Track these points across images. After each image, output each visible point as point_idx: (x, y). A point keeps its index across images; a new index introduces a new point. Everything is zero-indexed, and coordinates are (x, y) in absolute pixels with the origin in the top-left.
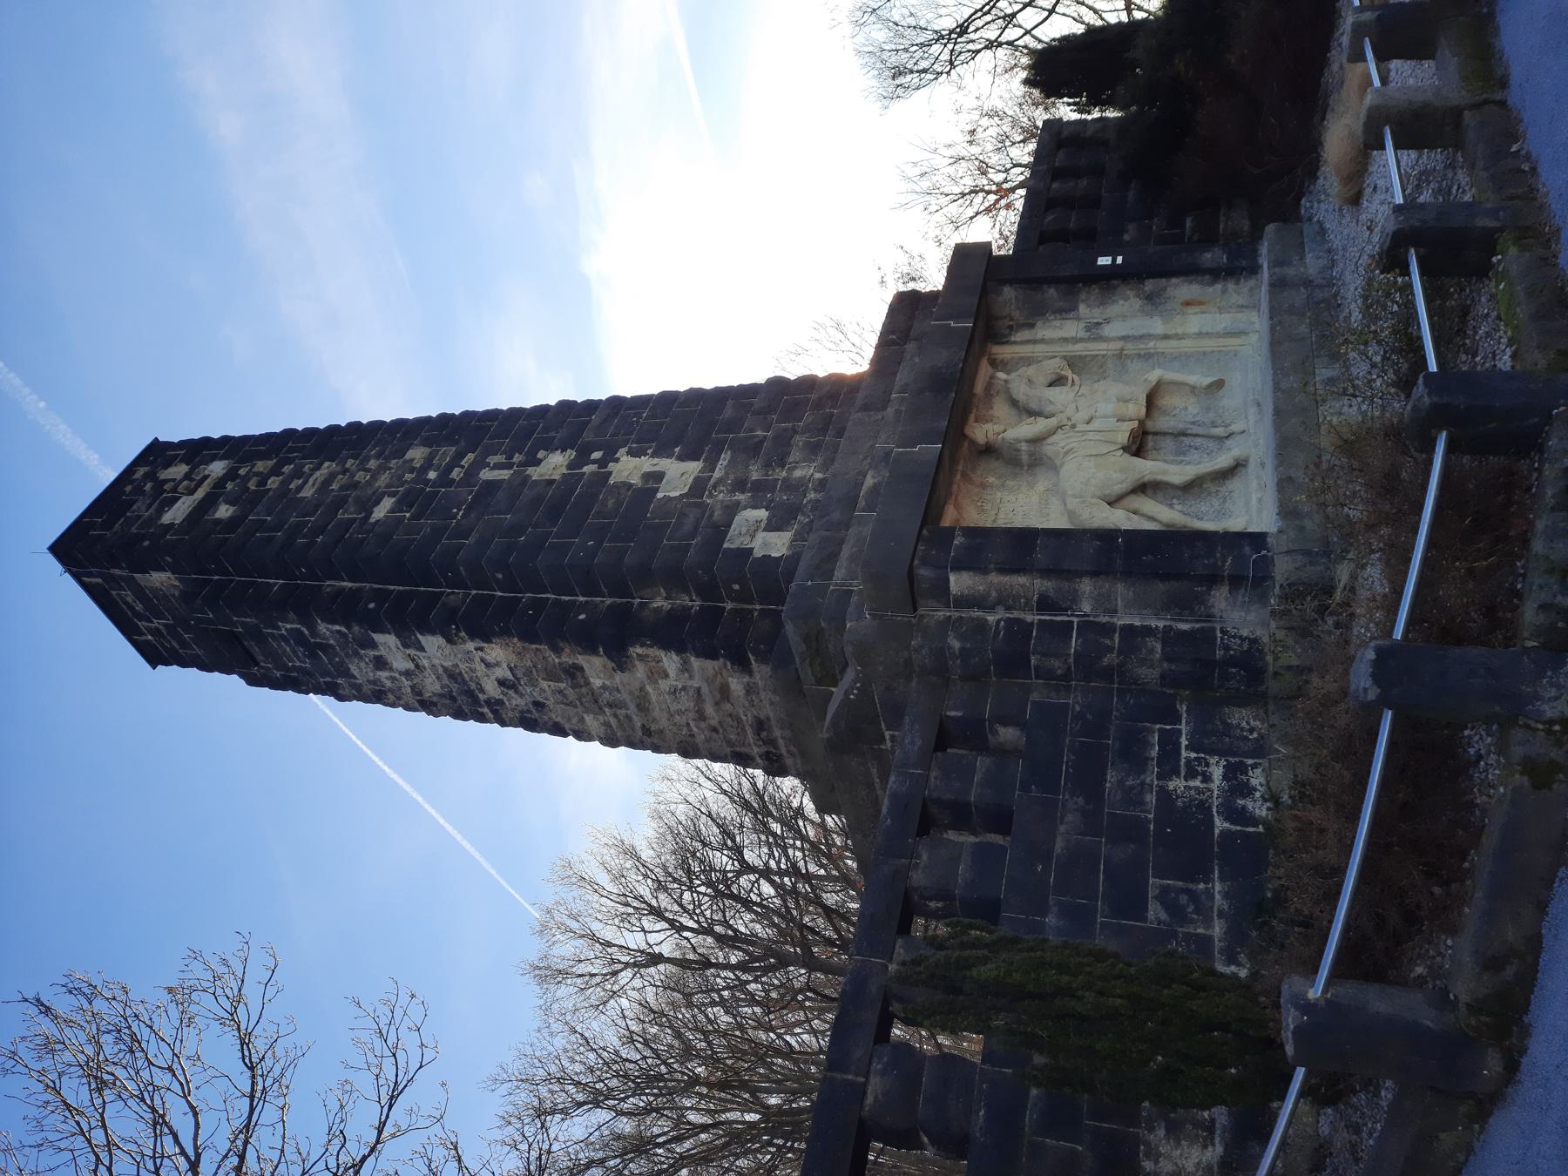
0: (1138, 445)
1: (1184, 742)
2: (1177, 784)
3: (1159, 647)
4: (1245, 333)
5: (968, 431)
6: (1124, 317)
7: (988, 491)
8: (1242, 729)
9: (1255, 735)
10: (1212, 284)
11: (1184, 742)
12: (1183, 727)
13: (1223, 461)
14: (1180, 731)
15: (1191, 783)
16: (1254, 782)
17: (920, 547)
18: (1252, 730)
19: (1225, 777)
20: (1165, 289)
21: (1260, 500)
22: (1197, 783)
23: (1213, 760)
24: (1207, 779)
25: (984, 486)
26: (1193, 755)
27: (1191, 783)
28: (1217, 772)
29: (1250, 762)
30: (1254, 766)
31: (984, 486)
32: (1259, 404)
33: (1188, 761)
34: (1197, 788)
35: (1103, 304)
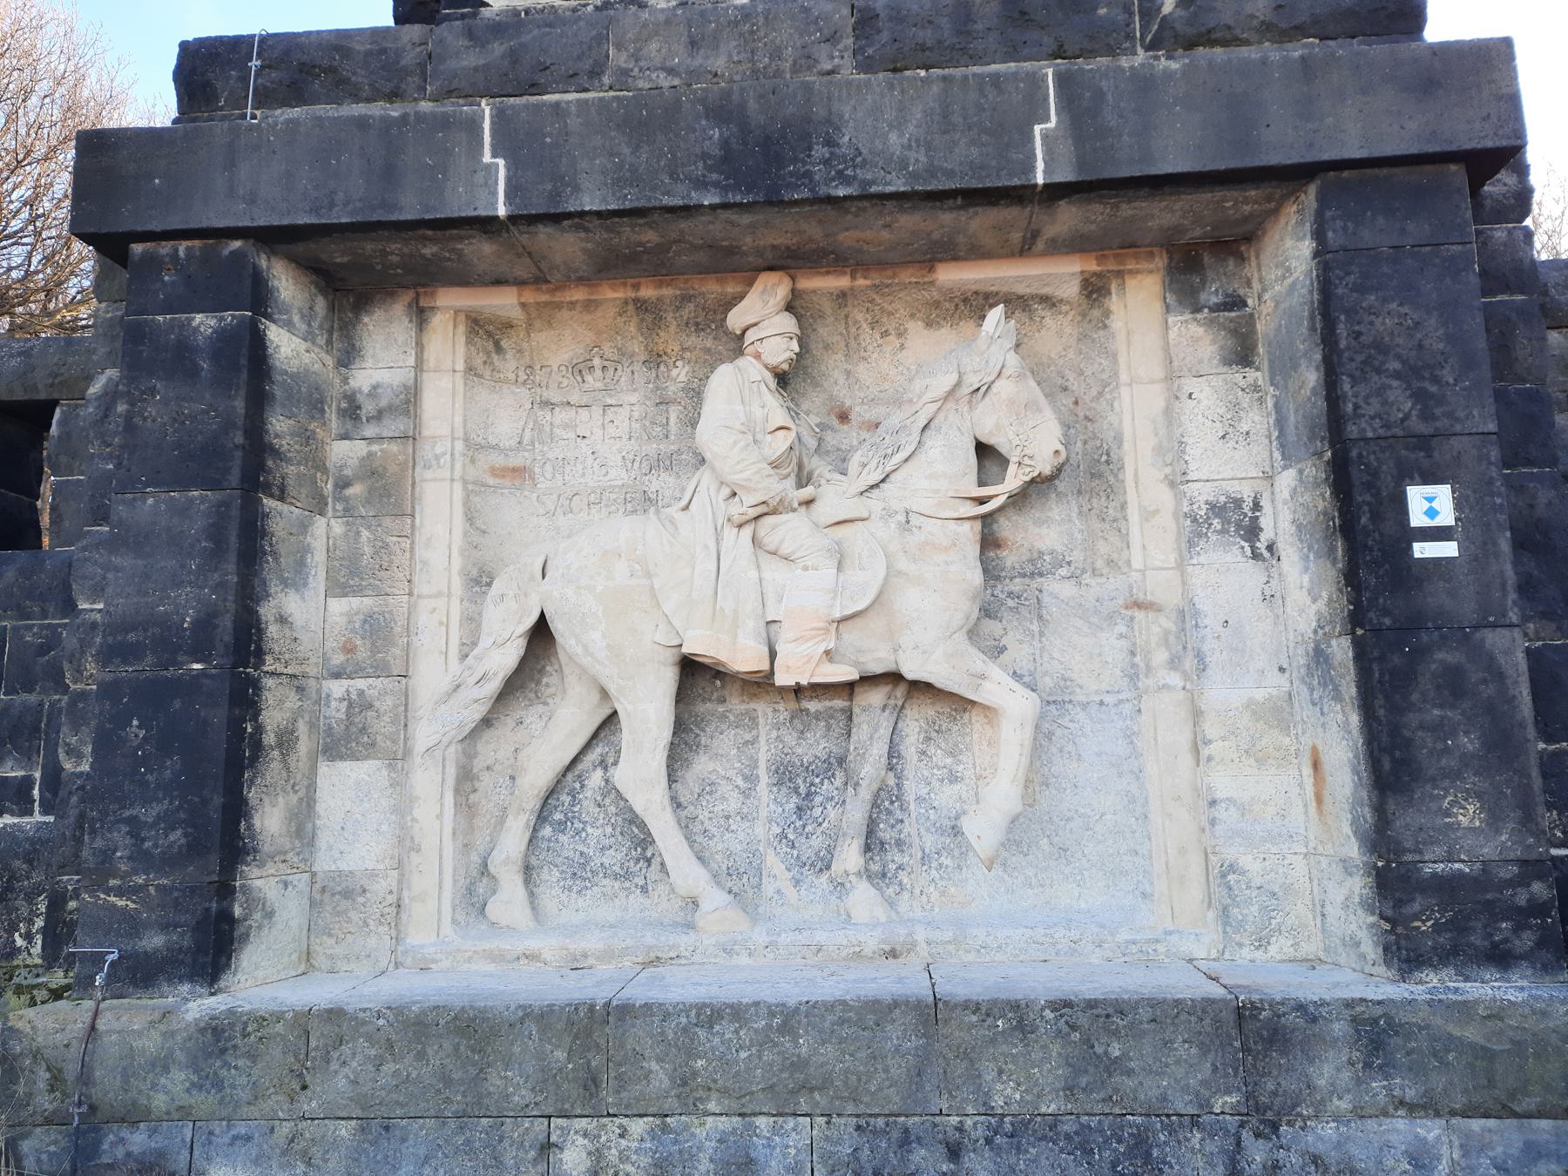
5: (766, 280)
7: (642, 373)
9: (19, 942)
10: (1354, 822)
12: (38, 817)
17: (182, 247)
20: (1338, 697)
21: (532, 957)
25: (656, 359)
31: (656, 359)
32: (893, 954)
35: (1299, 527)
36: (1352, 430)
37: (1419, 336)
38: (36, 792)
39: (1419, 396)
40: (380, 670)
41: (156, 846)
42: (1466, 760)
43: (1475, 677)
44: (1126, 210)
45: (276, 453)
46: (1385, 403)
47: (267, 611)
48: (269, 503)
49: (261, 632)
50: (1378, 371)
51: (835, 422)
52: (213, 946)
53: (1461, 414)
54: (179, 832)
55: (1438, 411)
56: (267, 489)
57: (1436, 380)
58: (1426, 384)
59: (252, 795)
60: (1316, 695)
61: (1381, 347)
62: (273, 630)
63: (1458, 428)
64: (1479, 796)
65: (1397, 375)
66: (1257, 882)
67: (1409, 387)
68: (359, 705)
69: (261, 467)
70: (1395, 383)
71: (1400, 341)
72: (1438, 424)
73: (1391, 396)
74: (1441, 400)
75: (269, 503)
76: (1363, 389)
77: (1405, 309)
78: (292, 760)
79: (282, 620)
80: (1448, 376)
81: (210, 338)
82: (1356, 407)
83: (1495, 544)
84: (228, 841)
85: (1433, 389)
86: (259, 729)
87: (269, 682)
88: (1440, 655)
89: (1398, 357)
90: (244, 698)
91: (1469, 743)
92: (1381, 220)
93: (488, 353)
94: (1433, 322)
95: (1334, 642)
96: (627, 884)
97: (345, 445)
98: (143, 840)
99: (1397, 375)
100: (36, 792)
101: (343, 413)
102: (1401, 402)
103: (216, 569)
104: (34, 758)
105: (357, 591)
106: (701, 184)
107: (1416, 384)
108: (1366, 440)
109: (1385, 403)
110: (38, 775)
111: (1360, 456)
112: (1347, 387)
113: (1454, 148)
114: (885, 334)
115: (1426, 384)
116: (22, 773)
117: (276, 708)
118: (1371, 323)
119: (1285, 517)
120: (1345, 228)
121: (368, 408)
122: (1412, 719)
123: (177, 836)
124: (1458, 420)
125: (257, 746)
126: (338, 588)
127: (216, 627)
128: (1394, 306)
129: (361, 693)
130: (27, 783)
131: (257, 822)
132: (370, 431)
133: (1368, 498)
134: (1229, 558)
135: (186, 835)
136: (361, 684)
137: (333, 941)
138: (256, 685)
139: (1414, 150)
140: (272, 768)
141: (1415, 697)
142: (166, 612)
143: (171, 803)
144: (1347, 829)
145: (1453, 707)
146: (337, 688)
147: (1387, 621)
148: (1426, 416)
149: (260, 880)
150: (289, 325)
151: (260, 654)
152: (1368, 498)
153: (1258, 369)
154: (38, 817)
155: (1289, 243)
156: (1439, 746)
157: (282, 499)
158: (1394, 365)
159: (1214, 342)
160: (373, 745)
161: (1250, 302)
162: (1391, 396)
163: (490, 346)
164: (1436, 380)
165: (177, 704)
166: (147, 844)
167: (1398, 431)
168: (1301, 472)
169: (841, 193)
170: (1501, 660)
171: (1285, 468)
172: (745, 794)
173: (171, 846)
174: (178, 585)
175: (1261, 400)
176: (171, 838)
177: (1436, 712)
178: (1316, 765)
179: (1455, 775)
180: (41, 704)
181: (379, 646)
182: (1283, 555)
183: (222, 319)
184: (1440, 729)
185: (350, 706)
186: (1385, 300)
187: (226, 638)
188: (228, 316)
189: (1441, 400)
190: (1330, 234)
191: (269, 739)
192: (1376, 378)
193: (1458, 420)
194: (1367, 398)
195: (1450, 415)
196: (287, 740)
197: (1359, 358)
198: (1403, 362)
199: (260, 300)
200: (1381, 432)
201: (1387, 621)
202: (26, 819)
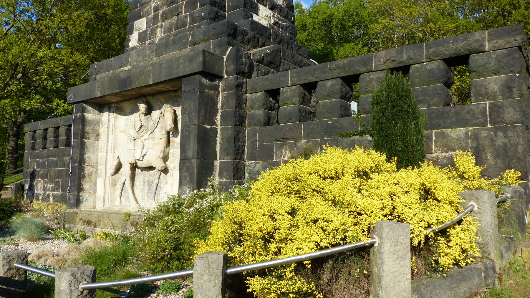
39: (189, 118)
45: (87, 132)
47: (85, 157)
48: (85, 140)
49: (84, 160)
52: (78, 202)
56: (86, 138)
59: (83, 183)
62: (87, 159)
65: (187, 114)
69: (84, 135)
78: (91, 178)
79: (89, 157)
84: (79, 189)
86: (84, 174)
90: (81, 169)
91: (188, 179)
117: (88, 170)
122: (183, 175)
125: (84, 176)
131: (84, 186)
138: (84, 167)
140: (87, 179)
148: (190, 122)
149: (84, 195)
150: (90, 113)
151: (84, 163)
157: (89, 139)
158: (187, 112)
164: (191, 115)
179: (186, 184)
191: (86, 175)
196: (90, 175)
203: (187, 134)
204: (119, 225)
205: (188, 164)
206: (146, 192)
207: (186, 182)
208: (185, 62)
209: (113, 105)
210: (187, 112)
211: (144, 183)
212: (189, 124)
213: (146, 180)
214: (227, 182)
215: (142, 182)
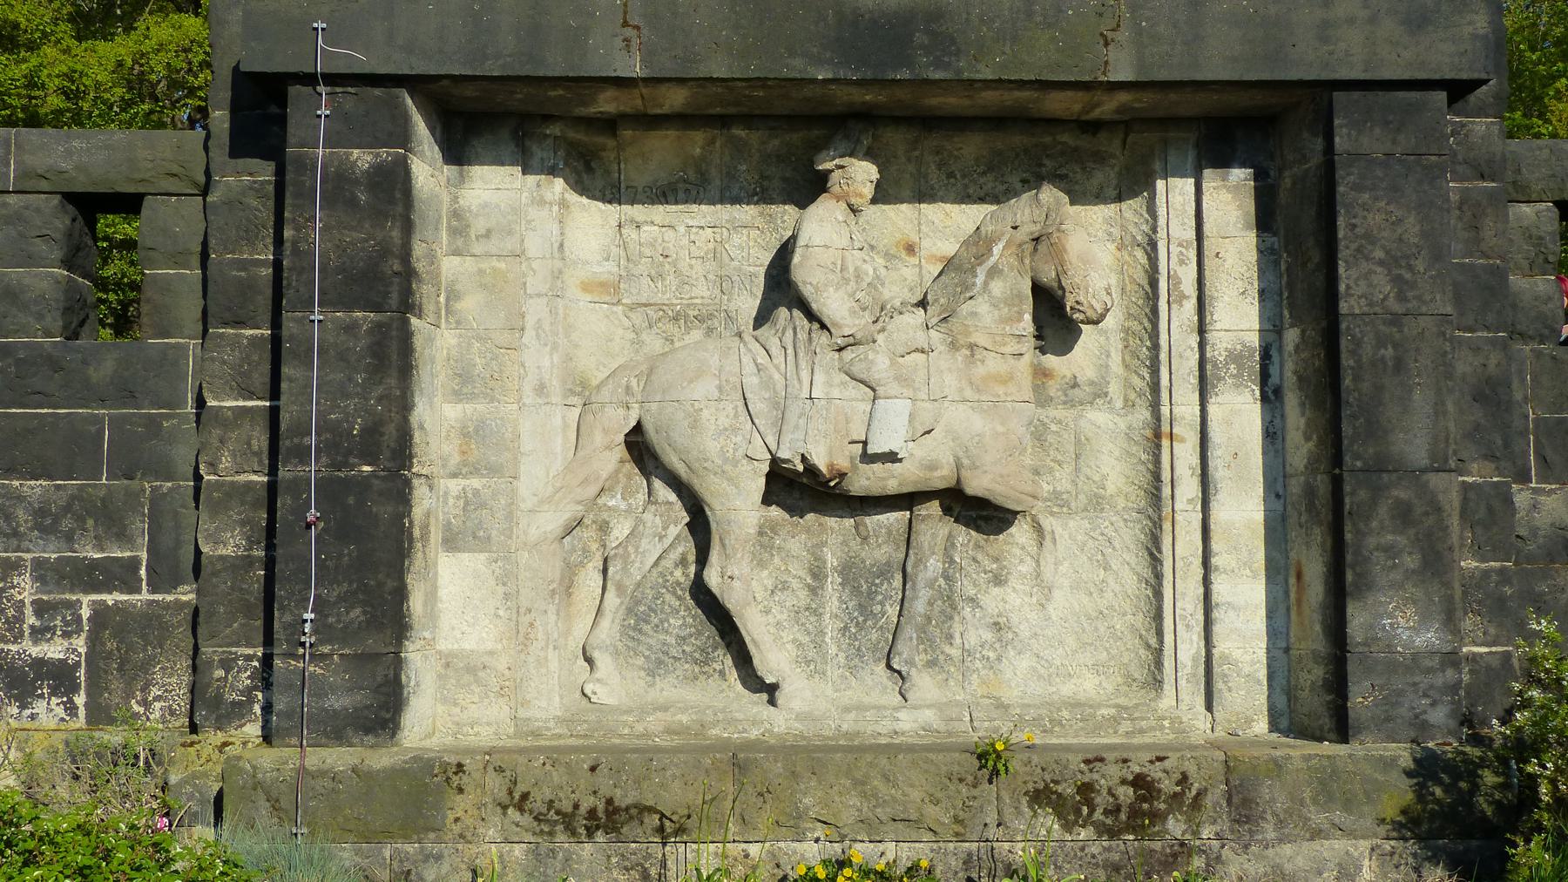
0: (797, 488)
1: (110, 599)
2: (25, 589)
3: (222, 551)
4: (1209, 707)
6: (1272, 435)
8: (145, 689)
9: (137, 708)
10: (1323, 623)
11: (110, 599)
12: (145, 595)
13: (771, 660)
14: (139, 591)
15: (29, 611)
16: (40, 707)
18: (145, 703)
19: (39, 663)
20: (1320, 523)
22: (31, 619)
23: (80, 644)
24: (38, 634)
26: (85, 613)
27: (29, 611)
28: (54, 650)
29: (80, 700)
30: (71, 709)
33: (74, 606)
34: (20, 619)
35: (1301, 379)
36: (1344, 307)
37: (1399, 231)
38: (143, 572)
39: (1397, 280)
40: (493, 470)
41: (339, 621)
42: (1409, 574)
43: (1418, 510)
44: (1173, 96)
46: (1370, 285)
49: (411, 437)
50: (1367, 259)
51: (903, 254)
53: (1428, 297)
54: (358, 611)
55: (1410, 294)
57: (1410, 268)
58: (1403, 272)
60: (1303, 519)
61: (1370, 238)
63: (1424, 309)
64: (1414, 603)
65: (1381, 263)
66: (1247, 670)
67: (1390, 271)
68: (471, 503)
70: (1379, 270)
71: (1385, 234)
72: (1410, 305)
73: (1375, 279)
74: (1413, 285)
75: (414, 321)
76: (1354, 273)
77: (1391, 208)
79: (422, 427)
80: (1420, 265)
81: (367, 172)
82: (1348, 287)
83: (1443, 403)
85: (1408, 276)
86: (411, 523)
87: (416, 482)
88: (1395, 493)
89: (1383, 247)
90: (401, 494)
91: (1411, 561)
92: (1377, 131)
93: (578, 173)
94: (1411, 219)
95: (1319, 477)
96: (706, 669)
97: (456, 260)
98: (327, 616)
99: (1381, 263)
100: (143, 572)
101: (454, 232)
102: (1383, 286)
103: (381, 383)
104: (139, 541)
105: (472, 397)
106: (819, 62)
107: (1396, 272)
108: (1354, 315)
109: (1370, 285)
110: (144, 555)
111: (1348, 328)
112: (1341, 270)
113: (1437, 77)
114: (951, 175)
115: (1403, 272)
116: (128, 554)
118: (1365, 218)
119: (1290, 366)
120: (1349, 135)
121: (479, 226)
122: (1372, 541)
123: (356, 612)
124: (1425, 303)
126: (458, 396)
127: (382, 435)
128: (1383, 204)
129: (476, 492)
130: (134, 564)
132: (478, 248)
133: (1351, 362)
134: (1240, 399)
135: (365, 613)
136: (476, 483)
137: (458, 710)
138: (408, 483)
139: (1406, 76)
141: (1374, 524)
142: (338, 421)
143: (350, 583)
144: (1318, 628)
145: (1401, 533)
146: (455, 486)
147: (1359, 464)
148: (1401, 298)
150: (422, 157)
151: (411, 457)
152: (1351, 362)
153: (1275, 235)
154: (145, 595)
155: (1306, 135)
156: (1390, 563)
157: (420, 317)
158: (1379, 254)
159: (1240, 207)
160: (489, 538)
161: (1272, 173)
162: (1375, 279)
163: (581, 167)
164: (1410, 268)
165: (351, 500)
166: (331, 620)
167: (1377, 309)
168: (1303, 332)
169: (938, 75)
170: (1441, 497)
171: (1292, 326)
172: (813, 591)
173: (352, 622)
174: (347, 396)
175: (1277, 263)
176: (352, 615)
177: (1390, 537)
178: (1299, 576)
180: (144, 491)
181: (487, 452)
182: (1286, 400)
183: (377, 155)
184: (1391, 551)
185: (467, 503)
186: (1376, 199)
187: (392, 445)
188: (383, 152)
189: (1413, 285)
190: (1337, 139)
191: (417, 533)
192: (1364, 264)
193: (1425, 303)
194: (1358, 279)
195: (1419, 298)
197: (1354, 246)
198: (1387, 252)
199: (403, 138)
200: (1366, 309)
201: (1359, 464)
202: (137, 597)
203: (1389, 352)
204: (931, 811)
205: (1401, 493)
206: (831, 627)
207: (1396, 576)
208: (1373, 20)
209: (555, 130)
210: (1379, 254)
211: (818, 574)
212: (1398, 308)
213: (831, 560)
214: (1486, 574)
215: (798, 570)
